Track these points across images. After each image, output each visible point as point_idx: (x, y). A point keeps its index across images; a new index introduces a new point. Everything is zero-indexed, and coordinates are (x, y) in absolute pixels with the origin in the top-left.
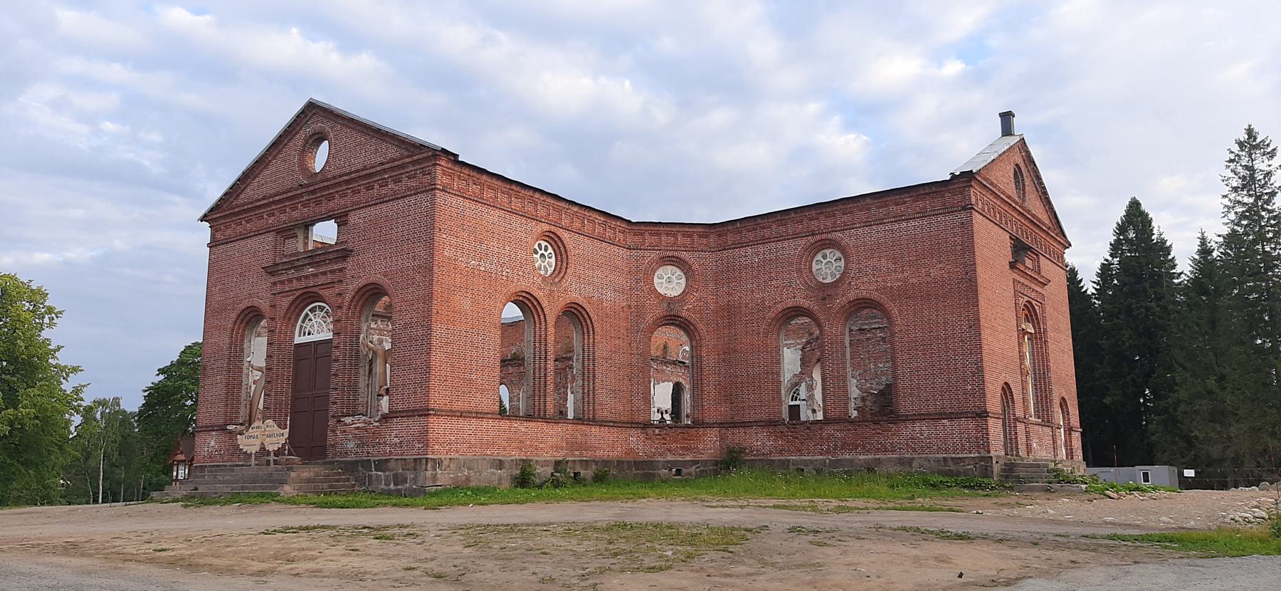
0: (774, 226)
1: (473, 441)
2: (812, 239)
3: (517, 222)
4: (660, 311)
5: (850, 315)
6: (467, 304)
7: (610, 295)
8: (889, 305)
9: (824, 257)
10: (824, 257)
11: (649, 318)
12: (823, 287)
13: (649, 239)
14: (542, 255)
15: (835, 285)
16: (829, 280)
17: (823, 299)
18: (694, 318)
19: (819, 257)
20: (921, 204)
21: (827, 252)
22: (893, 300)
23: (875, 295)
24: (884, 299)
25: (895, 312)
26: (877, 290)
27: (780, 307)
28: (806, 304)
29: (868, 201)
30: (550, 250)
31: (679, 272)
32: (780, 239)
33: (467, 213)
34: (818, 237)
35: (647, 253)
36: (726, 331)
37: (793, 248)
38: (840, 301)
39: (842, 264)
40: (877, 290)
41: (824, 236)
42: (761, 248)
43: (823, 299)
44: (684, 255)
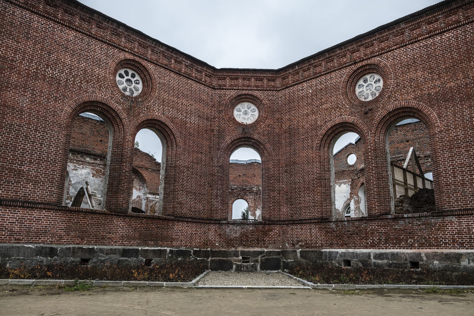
0: (323, 64)
1: (16, 229)
2: (354, 67)
3: (96, 46)
4: (237, 134)
5: (390, 125)
6: (24, 102)
7: (194, 119)
8: (427, 110)
9: (365, 81)
10: (365, 81)
11: (228, 139)
12: (363, 104)
13: (228, 82)
14: (128, 80)
15: (376, 101)
16: (370, 98)
17: (366, 113)
18: (262, 139)
19: (361, 82)
20: (454, 18)
21: (368, 77)
22: (432, 106)
23: (413, 103)
24: (422, 106)
25: (434, 115)
26: (415, 98)
27: (329, 125)
28: (351, 119)
29: (403, 26)
30: (130, 72)
31: (253, 107)
32: (329, 72)
33: (35, 25)
34: (360, 65)
35: (228, 92)
36: (288, 149)
37: (339, 77)
38: (380, 114)
39: (381, 84)
40: (415, 98)
41: (364, 63)
42: (314, 82)
43: (366, 113)
44: (256, 93)
